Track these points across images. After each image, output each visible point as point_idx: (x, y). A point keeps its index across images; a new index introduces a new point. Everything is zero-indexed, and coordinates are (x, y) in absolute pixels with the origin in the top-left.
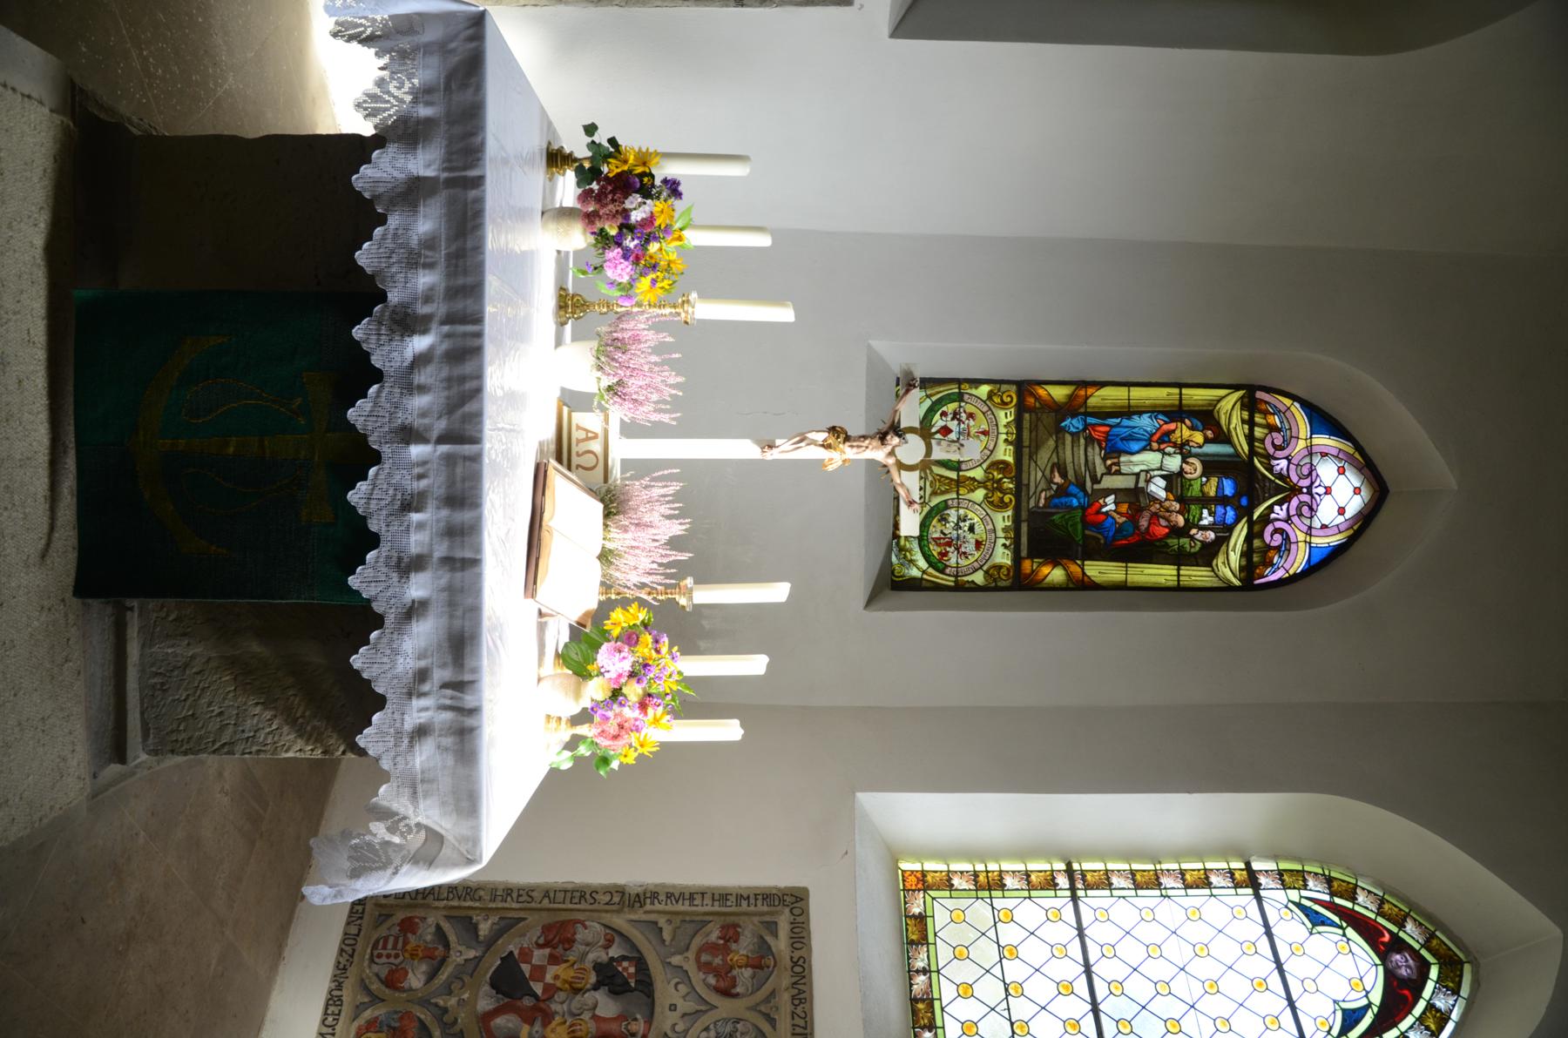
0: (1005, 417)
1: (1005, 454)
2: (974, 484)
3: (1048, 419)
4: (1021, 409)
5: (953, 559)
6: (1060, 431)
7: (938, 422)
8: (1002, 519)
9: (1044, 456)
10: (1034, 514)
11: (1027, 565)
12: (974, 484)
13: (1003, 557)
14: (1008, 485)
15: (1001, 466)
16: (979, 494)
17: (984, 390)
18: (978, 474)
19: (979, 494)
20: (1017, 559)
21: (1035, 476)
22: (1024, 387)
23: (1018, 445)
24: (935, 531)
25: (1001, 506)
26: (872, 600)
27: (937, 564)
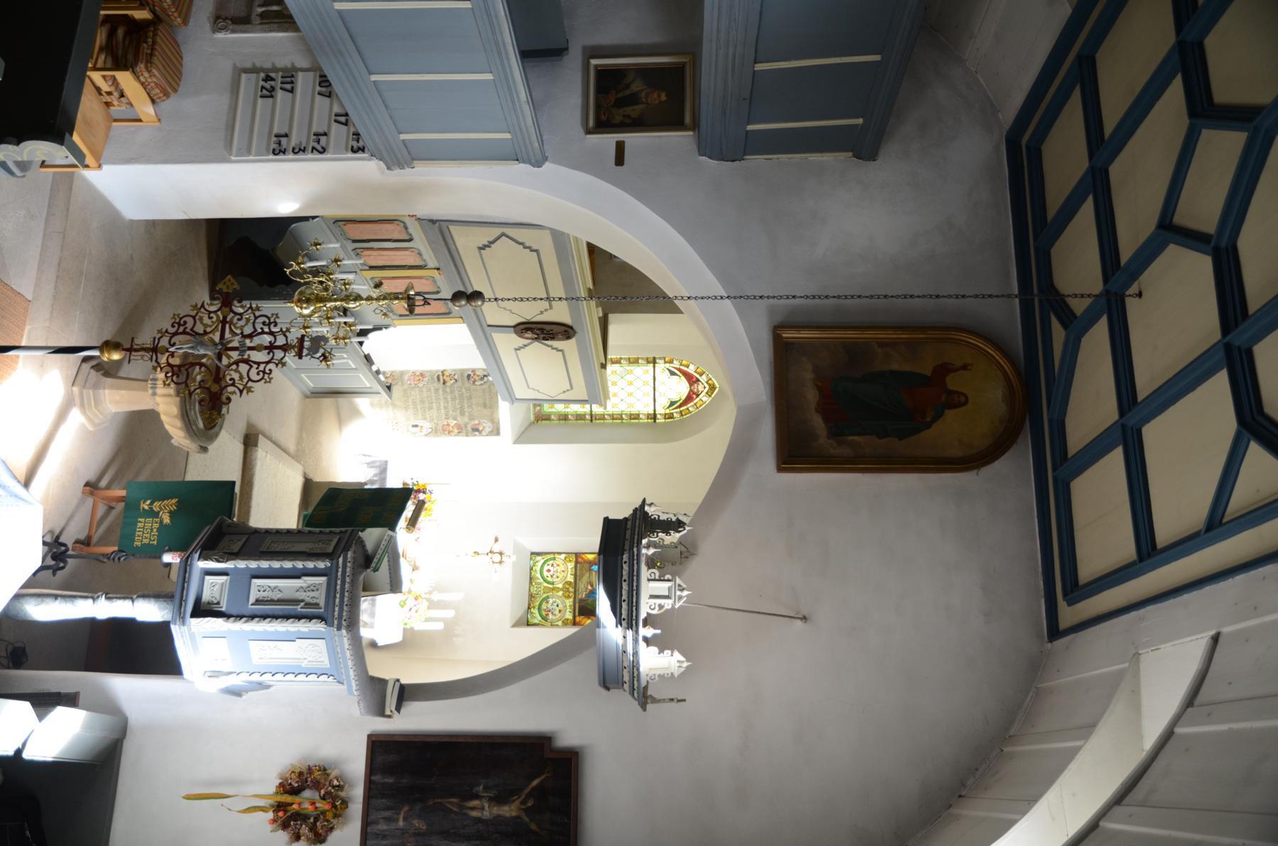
0: (571, 565)
1: (571, 579)
2: (558, 589)
3: (586, 566)
4: (577, 562)
5: (551, 616)
6: (590, 570)
7: (546, 568)
8: (569, 602)
9: (585, 579)
10: (581, 600)
11: (578, 619)
12: (558, 589)
13: (569, 616)
14: (571, 590)
15: (569, 583)
16: (561, 593)
17: (563, 556)
18: (560, 586)
19: (561, 593)
20: (574, 617)
21: (581, 586)
22: (577, 555)
23: (575, 576)
24: (544, 606)
25: (569, 597)
26: (515, 625)
27: (545, 619)
